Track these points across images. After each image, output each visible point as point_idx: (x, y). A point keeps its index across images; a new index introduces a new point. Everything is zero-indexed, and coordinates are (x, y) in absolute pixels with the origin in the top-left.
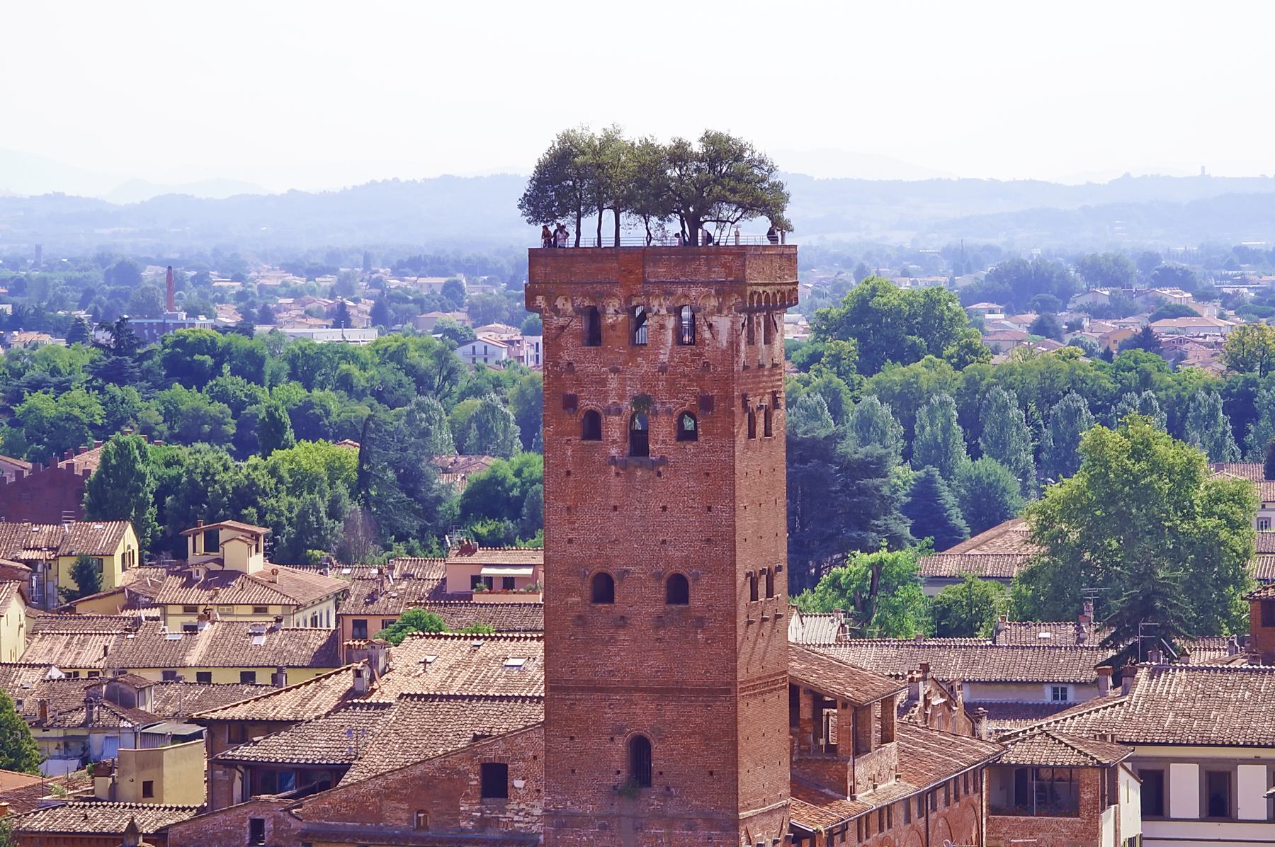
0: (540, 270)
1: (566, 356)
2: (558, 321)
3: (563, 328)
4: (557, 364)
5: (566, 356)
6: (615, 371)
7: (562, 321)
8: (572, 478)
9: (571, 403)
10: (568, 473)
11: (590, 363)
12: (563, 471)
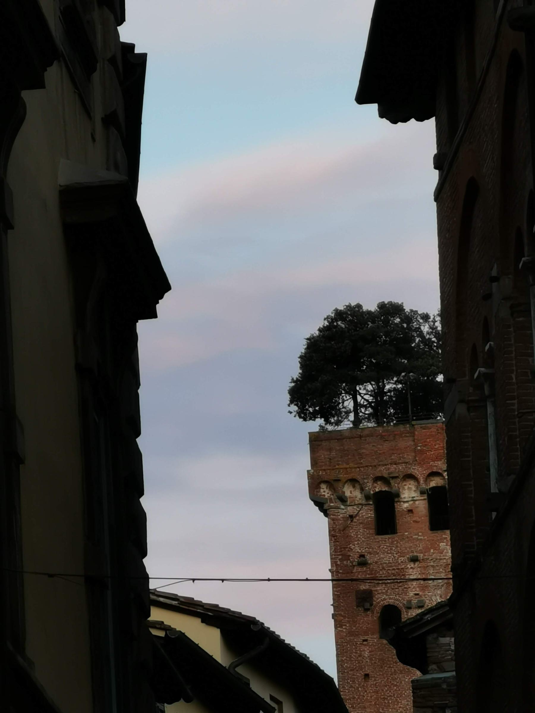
0: (323, 454)
1: (357, 549)
2: (344, 511)
3: (351, 517)
4: (347, 557)
5: (357, 549)
6: (414, 560)
7: (351, 510)
8: (371, 682)
9: (365, 599)
10: (367, 676)
11: (385, 553)
12: (360, 674)
